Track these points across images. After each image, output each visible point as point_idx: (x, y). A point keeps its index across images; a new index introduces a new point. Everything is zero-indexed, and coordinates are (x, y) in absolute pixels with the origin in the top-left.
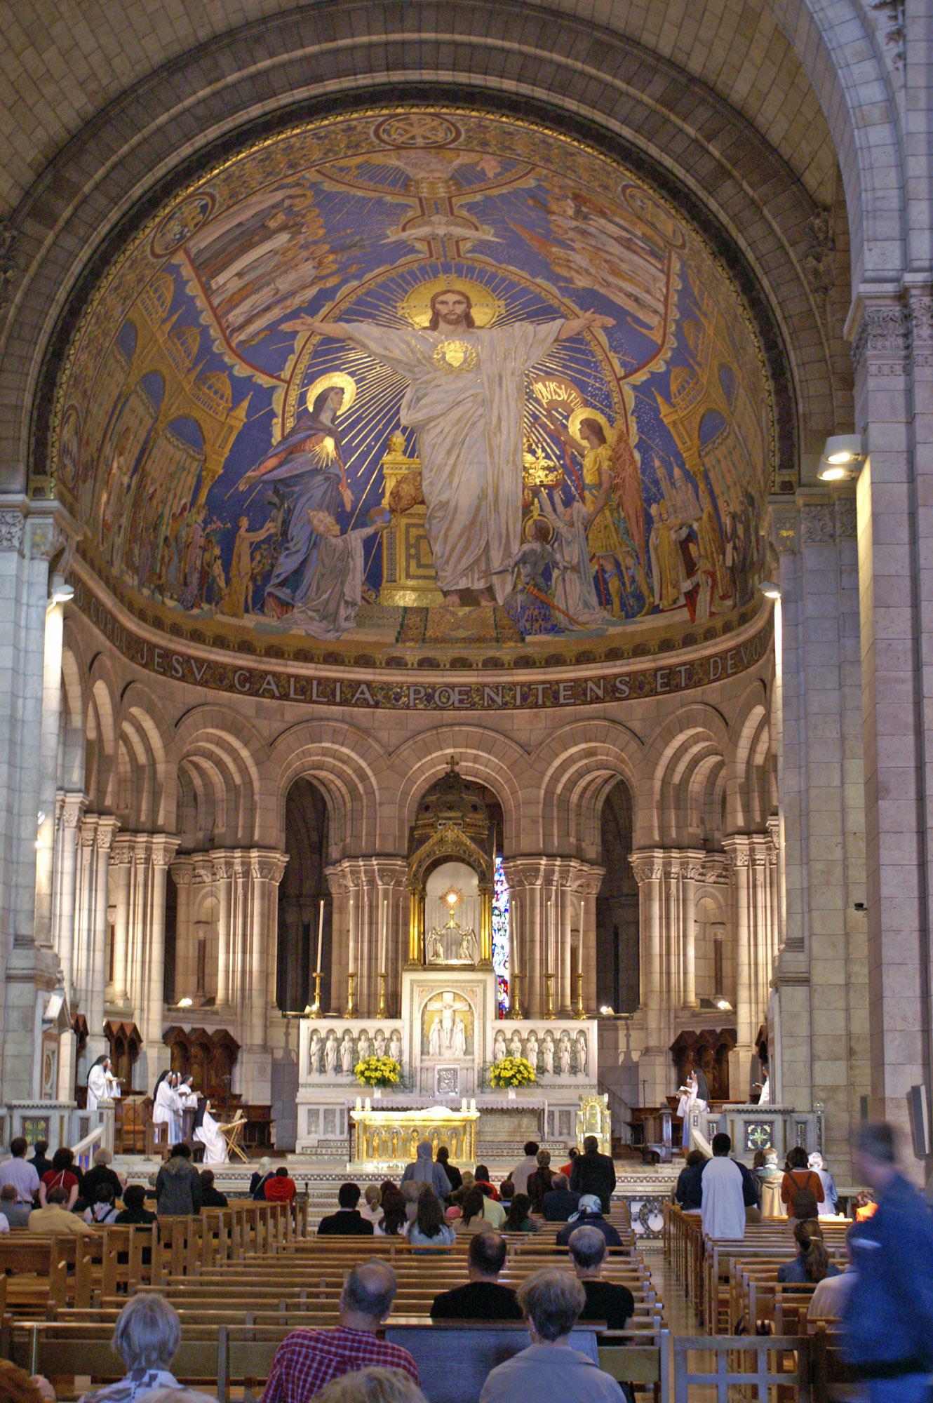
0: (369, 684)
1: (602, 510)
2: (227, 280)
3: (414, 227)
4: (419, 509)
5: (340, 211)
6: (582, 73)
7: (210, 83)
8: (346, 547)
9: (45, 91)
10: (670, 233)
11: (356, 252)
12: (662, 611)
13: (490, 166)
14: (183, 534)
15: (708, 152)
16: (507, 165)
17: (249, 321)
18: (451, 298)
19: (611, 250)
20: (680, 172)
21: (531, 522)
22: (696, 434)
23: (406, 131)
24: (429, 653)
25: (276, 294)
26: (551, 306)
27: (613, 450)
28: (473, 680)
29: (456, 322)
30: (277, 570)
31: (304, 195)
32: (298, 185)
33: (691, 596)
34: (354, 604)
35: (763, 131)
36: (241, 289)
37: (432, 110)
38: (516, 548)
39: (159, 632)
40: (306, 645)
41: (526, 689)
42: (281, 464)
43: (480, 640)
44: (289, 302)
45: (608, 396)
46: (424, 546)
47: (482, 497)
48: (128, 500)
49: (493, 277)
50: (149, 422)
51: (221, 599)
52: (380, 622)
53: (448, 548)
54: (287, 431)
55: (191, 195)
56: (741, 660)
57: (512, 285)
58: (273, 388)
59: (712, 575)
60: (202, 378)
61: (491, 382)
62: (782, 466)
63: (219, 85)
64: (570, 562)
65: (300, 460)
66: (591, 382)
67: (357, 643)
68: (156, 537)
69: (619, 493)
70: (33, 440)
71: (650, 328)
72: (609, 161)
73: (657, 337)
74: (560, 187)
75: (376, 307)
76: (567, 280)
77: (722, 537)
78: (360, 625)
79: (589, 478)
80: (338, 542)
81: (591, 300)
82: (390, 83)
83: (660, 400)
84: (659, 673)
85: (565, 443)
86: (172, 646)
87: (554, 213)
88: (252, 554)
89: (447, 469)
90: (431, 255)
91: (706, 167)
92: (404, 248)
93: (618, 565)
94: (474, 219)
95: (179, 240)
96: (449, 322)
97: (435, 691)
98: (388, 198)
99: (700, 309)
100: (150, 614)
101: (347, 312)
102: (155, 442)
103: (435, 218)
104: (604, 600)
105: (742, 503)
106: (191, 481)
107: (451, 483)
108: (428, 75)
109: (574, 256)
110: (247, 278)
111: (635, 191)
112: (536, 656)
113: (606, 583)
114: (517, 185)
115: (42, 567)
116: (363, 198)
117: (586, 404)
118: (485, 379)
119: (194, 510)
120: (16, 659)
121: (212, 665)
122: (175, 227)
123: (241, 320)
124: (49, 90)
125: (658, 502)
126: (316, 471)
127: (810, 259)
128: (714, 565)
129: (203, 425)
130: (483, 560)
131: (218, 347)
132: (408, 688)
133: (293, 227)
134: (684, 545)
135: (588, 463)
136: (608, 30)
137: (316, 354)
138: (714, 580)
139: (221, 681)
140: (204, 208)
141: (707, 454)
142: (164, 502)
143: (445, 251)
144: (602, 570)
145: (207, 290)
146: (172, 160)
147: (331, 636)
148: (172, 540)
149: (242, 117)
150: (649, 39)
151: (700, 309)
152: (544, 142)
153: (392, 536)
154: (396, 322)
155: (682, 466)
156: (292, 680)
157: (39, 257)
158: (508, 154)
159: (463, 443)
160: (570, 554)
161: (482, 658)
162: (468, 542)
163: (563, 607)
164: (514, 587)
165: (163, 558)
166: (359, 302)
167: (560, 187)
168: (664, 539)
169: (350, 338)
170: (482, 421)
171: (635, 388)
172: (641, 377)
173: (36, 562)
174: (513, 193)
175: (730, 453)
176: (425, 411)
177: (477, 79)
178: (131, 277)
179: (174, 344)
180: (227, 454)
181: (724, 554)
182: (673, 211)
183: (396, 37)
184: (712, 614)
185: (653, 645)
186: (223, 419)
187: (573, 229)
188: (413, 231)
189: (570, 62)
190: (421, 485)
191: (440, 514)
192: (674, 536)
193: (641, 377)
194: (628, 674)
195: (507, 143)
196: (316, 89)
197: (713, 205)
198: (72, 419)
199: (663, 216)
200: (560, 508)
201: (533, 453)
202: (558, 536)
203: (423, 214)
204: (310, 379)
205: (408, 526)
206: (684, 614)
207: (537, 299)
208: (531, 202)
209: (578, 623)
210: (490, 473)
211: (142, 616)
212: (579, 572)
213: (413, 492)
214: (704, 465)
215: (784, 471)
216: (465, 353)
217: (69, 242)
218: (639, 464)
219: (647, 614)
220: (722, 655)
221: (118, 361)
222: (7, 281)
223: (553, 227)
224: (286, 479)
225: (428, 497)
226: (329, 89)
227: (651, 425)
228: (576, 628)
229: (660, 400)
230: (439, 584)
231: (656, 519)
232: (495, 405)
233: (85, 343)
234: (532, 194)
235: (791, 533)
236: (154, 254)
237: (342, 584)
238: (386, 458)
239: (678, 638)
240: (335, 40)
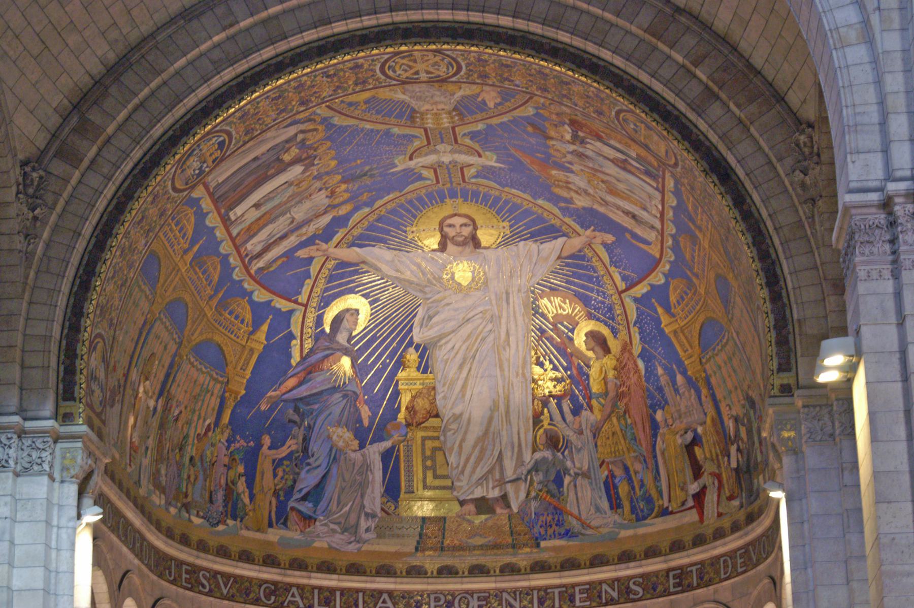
1: (609, 416)
2: (245, 212)
3: (420, 156)
4: (433, 422)
5: (350, 143)
7: (224, 29)
8: (365, 460)
9: (70, 41)
10: (662, 153)
11: (367, 181)
12: (672, 513)
13: (490, 97)
14: (208, 453)
15: (695, 76)
17: (266, 249)
18: (457, 221)
19: (608, 171)
20: (670, 96)
21: (541, 431)
22: (697, 342)
23: (411, 67)
24: (448, 561)
25: (292, 222)
26: (553, 226)
27: (618, 360)
28: (492, 585)
29: (463, 244)
30: (299, 486)
31: (316, 130)
32: (308, 120)
33: (699, 497)
34: (373, 516)
35: (746, 55)
36: (260, 219)
37: (434, 47)
38: (528, 457)
39: (186, 549)
40: (328, 557)
41: (543, 593)
42: (300, 384)
43: (496, 546)
44: (304, 230)
45: (611, 309)
46: (439, 457)
47: (494, 408)
48: (155, 423)
49: (497, 199)
50: (173, 347)
51: (246, 514)
52: (399, 532)
54: (306, 351)
55: (209, 133)
56: (750, 559)
57: (516, 207)
58: (291, 312)
59: (718, 477)
60: (222, 305)
62: (780, 370)
63: (232, 31)
64: (580, 469)
65: (319, 379)
66: (594, 295)
67: (379, 554)
68: (182, 456)
69: (625, 401)
70: (62, 368)
71: (648, 243)
72: (602, 88)
73: (655, 251)
74: (557, 114)
75: (388, 232)
76: (570, 201)
77: (726, 440)
78: (379, 536)
79: (596, 387)
80: (357, 456)
82: (393, 23)
83: (660, 310)
84: (671, 574)
85: (571, 355)
86: (199, 562)
87: (552, 138)
88: (274, 470)
89: (460, 383)
90: (438, 182)
91: (694, 90)
92: (411, 176)
93: (626, 469)
94: (477, 147)
95: (199, 175)
96: (457, 244)
97: (454, 599)
98: (396, 130)
99: (693, 222)
100: (177, 532)
101: (361, 237)
102: (179, 366)
103: (441, 147)
104: (615, 504)
105: (743, 406)
106: (215, 402)
107: (463, 396)
109: (573, 178)
110: (264, 209)
111: (629, 116)
112: (551, 560)
113: (615, 487)
114: (517, 113)
115: (72, 490)
116: (372, 131)
117: (590, 316)
118: (493, 297)
119: (218, 430)
120: (47, 580)
121: (238, 579)
122: (194, 163)
123: (259, 248)
124: (73, 39)
125: (663, 408)
126: (334, 389)
127: (797, 172)
128: (719, 467)
129: (224, 348)
130: (497, 469)
131: (237, 275)
132: (429, 596)
133: (306, 159)
134: (689, 448)
135: (594, 372)
137: (331, 278)
138: (720, 482)
139: (247, 595)
140: (221, 145)
141: (708, 360)
142: (189, 423)
143: (450, 177)
144: (612, 475)
145: (226, 222)
146: (191, 101)
147: (352, 547)
148: (197, 459)
149: (255, 59)
151: (693, 222)
152: (540, 72)
153: (409, 450)
154: (406, 245)
155: (684, 373)
156: (316, 592)
157: (65, 195)
158: (507, 84)
159: (474, 357)
160: (581, 460)
161: (499, 564)
162: (483, 451)
163: (576, 512)
164: (527, 497)
165: (189, 477)
166: (371, 228)
167: (557, 114)
169: (364, 262)
170: (492, 337)
171: (636, 300)
172: (641, 289)
173: (66, 485)
174: (514, 121)
176: (436, 329)
177: (475, 17)
178: (153, 211)
179: (196, 273)
181: (729, 456)
182: (665, 133)
184: (720, 515)
185: (665, 545)
186: (244, 344)
187: (572, 153)
188: (419, 160)
190: (435, 399)
191: (454, 426)
192: (679, 441)
193: (641, 289)
194: (642, 576)
195: (506, 75)
196: (324, 32)
197: (702, 125)
198: (100, 346)
199: (656, 138)
201: (541, 365)
202: (568, 444)
203: (429, 143)
204: (326, 302)
205: (424, 439)
206: (692, 516)
207: (540, 219)
208: (530, 129)
209: (589, 526)
211: (169, 534)
212: (589, 478)
213: (427, 406)
214: (705, 371)
215: (782, 375)
216: (473, 272)
217: (94, 180)
218: (643, 372)
219: (656, 517)
220: (732, 554)
221: (142, 291)
222: (35, 218)
223: (551, 151)
224: (306, 397)
225: (442, 411)
226: (336, 30)
228: (589, 532)
230: (455, 493)
231: (662, 425)
232: (504, 321)
233: (110, 275)
235: (792, 434)
236: (175, 189)
237: (362, 496)
238: (401, 374)
239: (688, 538)
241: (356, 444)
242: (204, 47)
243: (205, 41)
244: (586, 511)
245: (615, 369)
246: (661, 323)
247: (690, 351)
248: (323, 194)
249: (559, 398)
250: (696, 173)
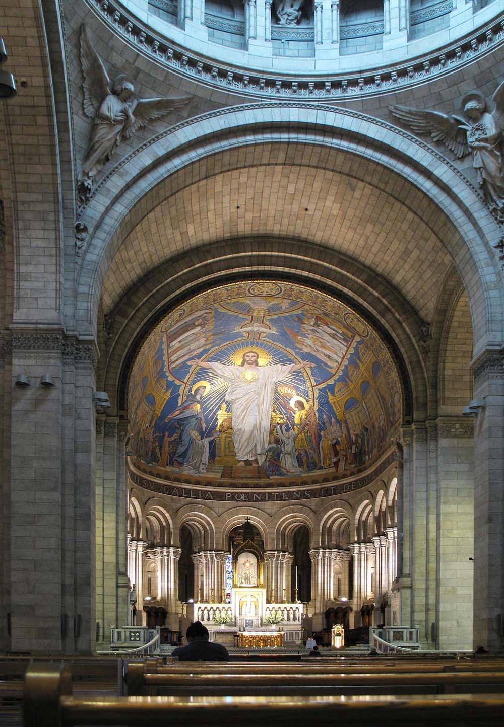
2: (175, 344)
6: (334, 271)
11: (222, 336)
17: (177, 360)
18: (252, 354)
20: (370, 308)
23: (261, 289)
38: (266, 446)
44: (192, 353)
45: (307, 393)
47: (255, 426)
53: (241, 445)
58: (181, 385)
60: (158, 380)
61: (262, 386)
66: (301, 387)
75: (222, 357)
80: (200, 442)
81: (307, 357)
83: (329, 394)
89: (242, 417)
91: (381, 307)
92: (239, 335)
98: (240, 316)
110: (181, 344)
117: (298, 395)
122: (170, 321)
123: (175, 359)
124: (128, 266)
126: (193, 416)
131: (165, 369)
136: (344, 254)
145: (168, 347)
150: (362, 259)
153: (220, 441)
154: (228, 363)
155: (335, 418)
168: (326, 443)
169: (211, 368)
171: (319, 389)
172: (323, 385)
175: (358, 413)
177: (293, 271)
180: (162, 409)
187: (311, 330)
189: (330, 266)
192: (330, 442)
197: (383, 321)
199: (361, 325)
201: (275, 412)
202: (283, 442)
204: (194, 383)
205: (226, 437)
207: (286, 356)
208: (296, 319)
210: (258, 418)
218: (317, 417)
227: (324, 402)
229: (329, 394)
234: (298, 316)
238: (219, 412)
240: (239, 253)
241: (199, 437)
243: (180, 272)
245: (306, 415)
246: (328, 398)
247: (340, 410)
250: (377, 339)
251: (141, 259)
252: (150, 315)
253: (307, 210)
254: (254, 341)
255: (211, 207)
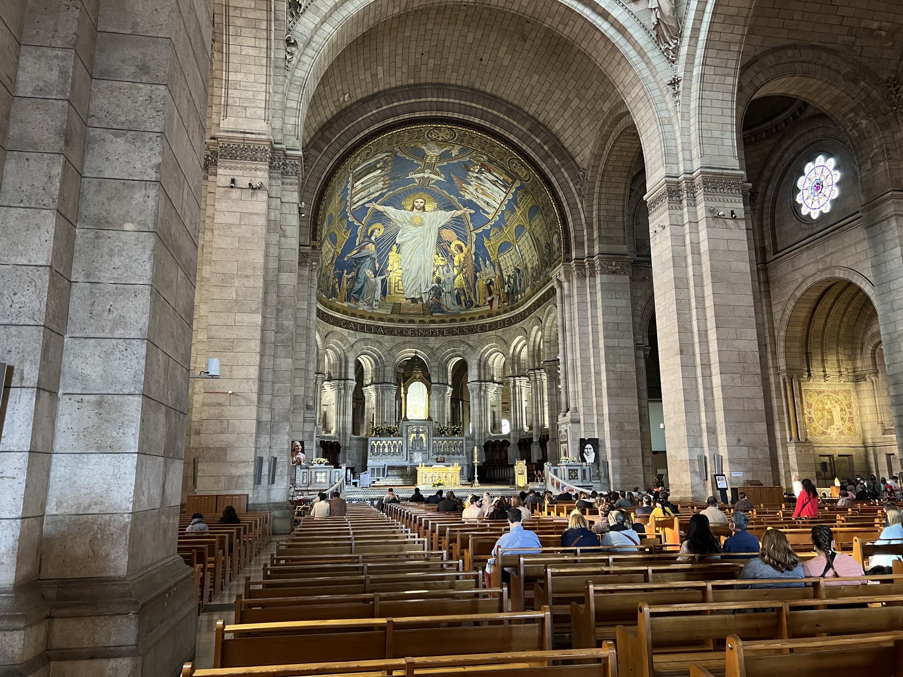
0: (382, 327)
2: (358, 185)
7: (377, 108)
13: (455, 152)
16: (461, 151)
18: (420, 200)
20: (533, 154)
24: (402, 318)
29: (420, 209)
33: (491, 302)
45: (466, 237)
46: (400, 282)
49: (436, 194)
57: (442, 197)
63: (379, 110)
71: (488, 214)
75: (395, 202)
76: (464, 196)
79: (456, 264)
87: (469, 171)
91: (543, 153)
92: (412, 180)
104: (459, 303)
106: (332, 255)
108: (450, 115)
110: (364, 185)
111: (515, 161)
117: (458, 239)
126: (368, 256)
134: (488, 286)
135: (456, 259)
136: (511, 104)
138: (500, 298)
145: (353, 187)
147: (370, 311)
150: (526, 108)
154: (400, 207)
155: (490, 260)
168: (481, 284)
183: (441, 100)
197: (544, 166)
199: (524, 169)
200: (445, 273)
201: (438, 254)
204: (370, 225)
206: (489, 308)
239: (486, 315)
242: (369, 114)
244: (449, 305)
248: (383, 183)
249: (443, 266)
251: (335, 98)
252: (341, 152)
253: (481, 60)
254: (424, 188)
255: (400, 51)
